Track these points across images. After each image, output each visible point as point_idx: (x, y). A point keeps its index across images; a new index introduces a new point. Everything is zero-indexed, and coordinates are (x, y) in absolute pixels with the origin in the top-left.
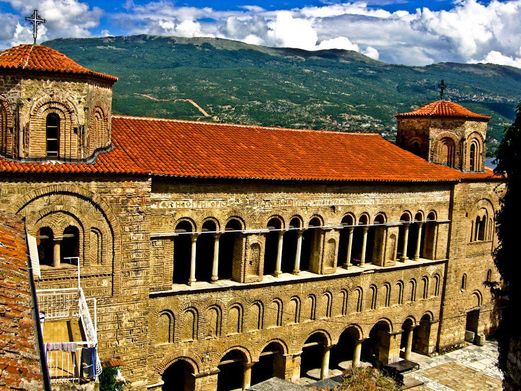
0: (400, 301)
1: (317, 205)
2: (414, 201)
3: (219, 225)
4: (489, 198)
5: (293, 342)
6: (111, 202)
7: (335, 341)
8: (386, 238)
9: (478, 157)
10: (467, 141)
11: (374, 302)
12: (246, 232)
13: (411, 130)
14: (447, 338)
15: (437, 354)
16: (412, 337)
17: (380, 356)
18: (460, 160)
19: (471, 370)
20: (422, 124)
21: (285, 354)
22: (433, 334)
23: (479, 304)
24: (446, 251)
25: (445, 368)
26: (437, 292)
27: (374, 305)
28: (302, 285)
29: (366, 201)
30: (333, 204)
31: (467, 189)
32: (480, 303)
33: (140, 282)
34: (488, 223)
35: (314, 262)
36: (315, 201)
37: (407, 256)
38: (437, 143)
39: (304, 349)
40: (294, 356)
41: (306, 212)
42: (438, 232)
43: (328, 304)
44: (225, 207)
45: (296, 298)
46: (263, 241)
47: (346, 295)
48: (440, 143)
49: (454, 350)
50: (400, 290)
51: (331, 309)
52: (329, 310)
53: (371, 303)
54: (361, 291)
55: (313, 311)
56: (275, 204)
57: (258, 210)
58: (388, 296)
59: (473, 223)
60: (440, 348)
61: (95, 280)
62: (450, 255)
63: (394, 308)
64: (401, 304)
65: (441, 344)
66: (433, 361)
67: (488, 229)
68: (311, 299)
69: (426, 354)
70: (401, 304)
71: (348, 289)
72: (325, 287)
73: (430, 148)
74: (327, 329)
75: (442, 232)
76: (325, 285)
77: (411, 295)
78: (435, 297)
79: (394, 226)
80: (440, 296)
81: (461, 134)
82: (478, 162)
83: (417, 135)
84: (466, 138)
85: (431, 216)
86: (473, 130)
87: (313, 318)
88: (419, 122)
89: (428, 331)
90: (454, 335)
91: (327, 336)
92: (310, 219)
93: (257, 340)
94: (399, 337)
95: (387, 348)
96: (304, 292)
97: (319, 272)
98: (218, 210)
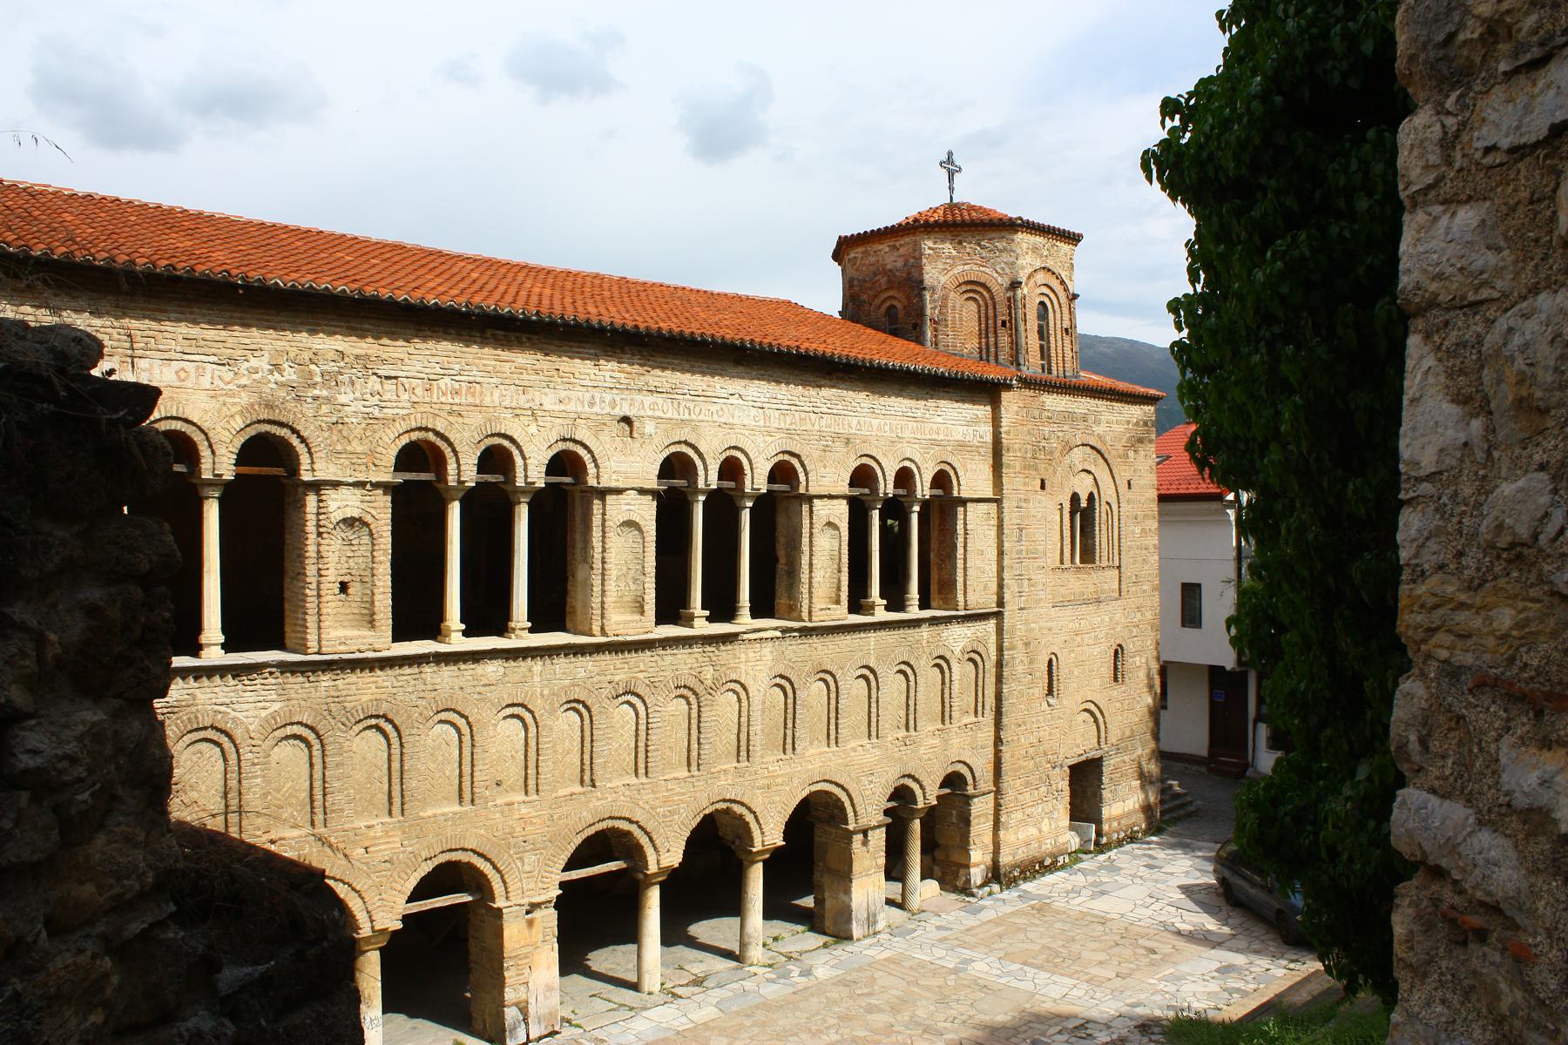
0: (872, 728)
1: (571, 407)
2: (887, 428)
3: (210, 446)
4: (1099, 446)
5: (520, 858)
7: (673, 856)
8: (811, 534)
9: (1059, 336)
10: (1025, 291)
11: (789, 732)
12: (321, 475)
13: (875, 274)
14: (1019, 842)
15: (996, 887)
16: (918, 843)
17: (828, 904)
18: (1012, 343)
19: (1097, 916)
20: (902, 251)
21: (500, 903)
22: (981, 830)
23: (1099, 742)
24: (994, 587)
25: (1018, 920)
26: (980, 704)
27: (789, 740)
28: (537, 666)
29: (737, 413)
31: (1036, 413)
32: (1103, 740)
34: (1104, 515)
35: (575, 600)
36: (563, 394)
37: (882, 596)
38: (945, 298)
39: (562, 885)
41: (533, 429)
42: (966, 530)
43: (637, 735)
44: (231, 386)
45: (519, 711)
46: (380, 511)
47: (695, 706)
48: (956, 299)
50: (870, 697)
51: (647, 751)
52: (642, 756)
53: (782, 735)
54: (743, 696)
55: (587, 757)
56: (419, 391)
57: (358, 406)
58: (833, 715)
59: (1061, 509)
60: (1002, 871)
62: (1007, 597)
63: (854, 750)
64: (874, 740)
65: (1005, 859)
66: (983, 908)
67: (1104, 532)
68: (573, 716)
69: (966, 890)
70: (874, 740)
71: (699, 689)
72: (620, 677)
73: (928, 312)
74: (638, 816)
75: (975, 526)
76: (619, 669)
77: (903, 713)
78: (975, 720)
79: (831, 497)
80: (989, 717)
81: (1007, 271)
82: (1060, 351)
83: (891, 285)
84: (1024, 280)
85: (941, 480)
86: (1038, 264)
87: (587, 778)
88: (894, 248)
89: (966, 821)
91: (644, 840)
92: (551, 453)
93: (386, 855)
94: (878, 838)
95: (844, 876)
96: (546, 692)
97: (596, 628)
98: (203, 395)
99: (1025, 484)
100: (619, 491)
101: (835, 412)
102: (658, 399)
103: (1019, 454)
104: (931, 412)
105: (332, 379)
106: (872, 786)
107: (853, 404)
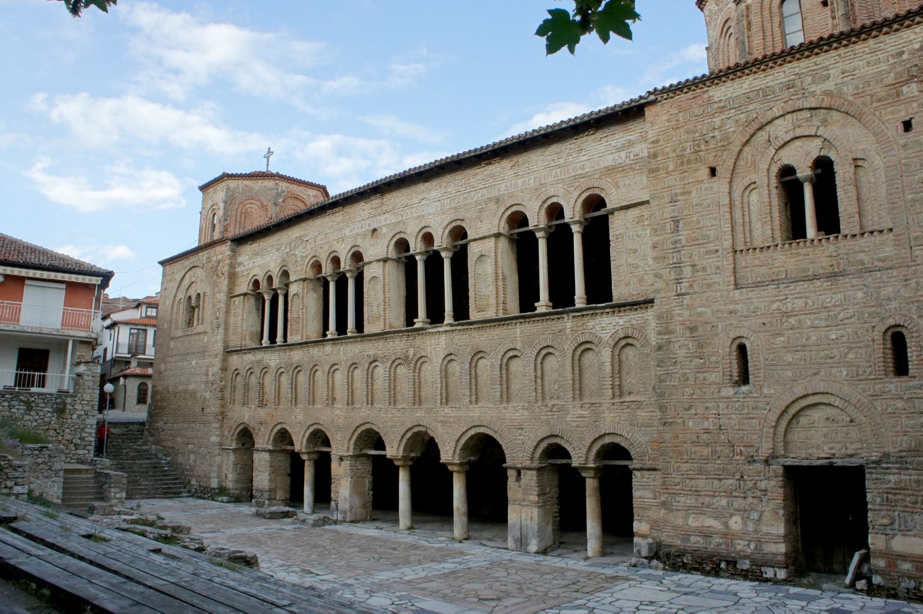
1: (354, 232)
2: (532, 181)
6: (211, 268)
28: (342, 348)
30: (375, 226)
33: (219, 337)
40: (341, 459)
41: (343, 246)
49: (733, 576)
61: (201, 336)
90: (727, 527)
93: (298, 420)
99: (681, 179)
100: (370, 263)
101: (487, 185)
102: (387, 215)
103: (671, 155)
104: (574, 156)
105: (295, 248)
106: (522, 437)
107: (502, 175)
